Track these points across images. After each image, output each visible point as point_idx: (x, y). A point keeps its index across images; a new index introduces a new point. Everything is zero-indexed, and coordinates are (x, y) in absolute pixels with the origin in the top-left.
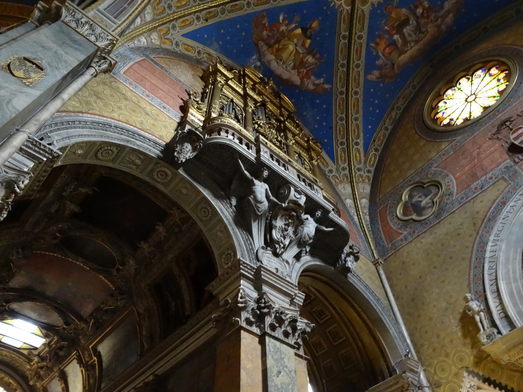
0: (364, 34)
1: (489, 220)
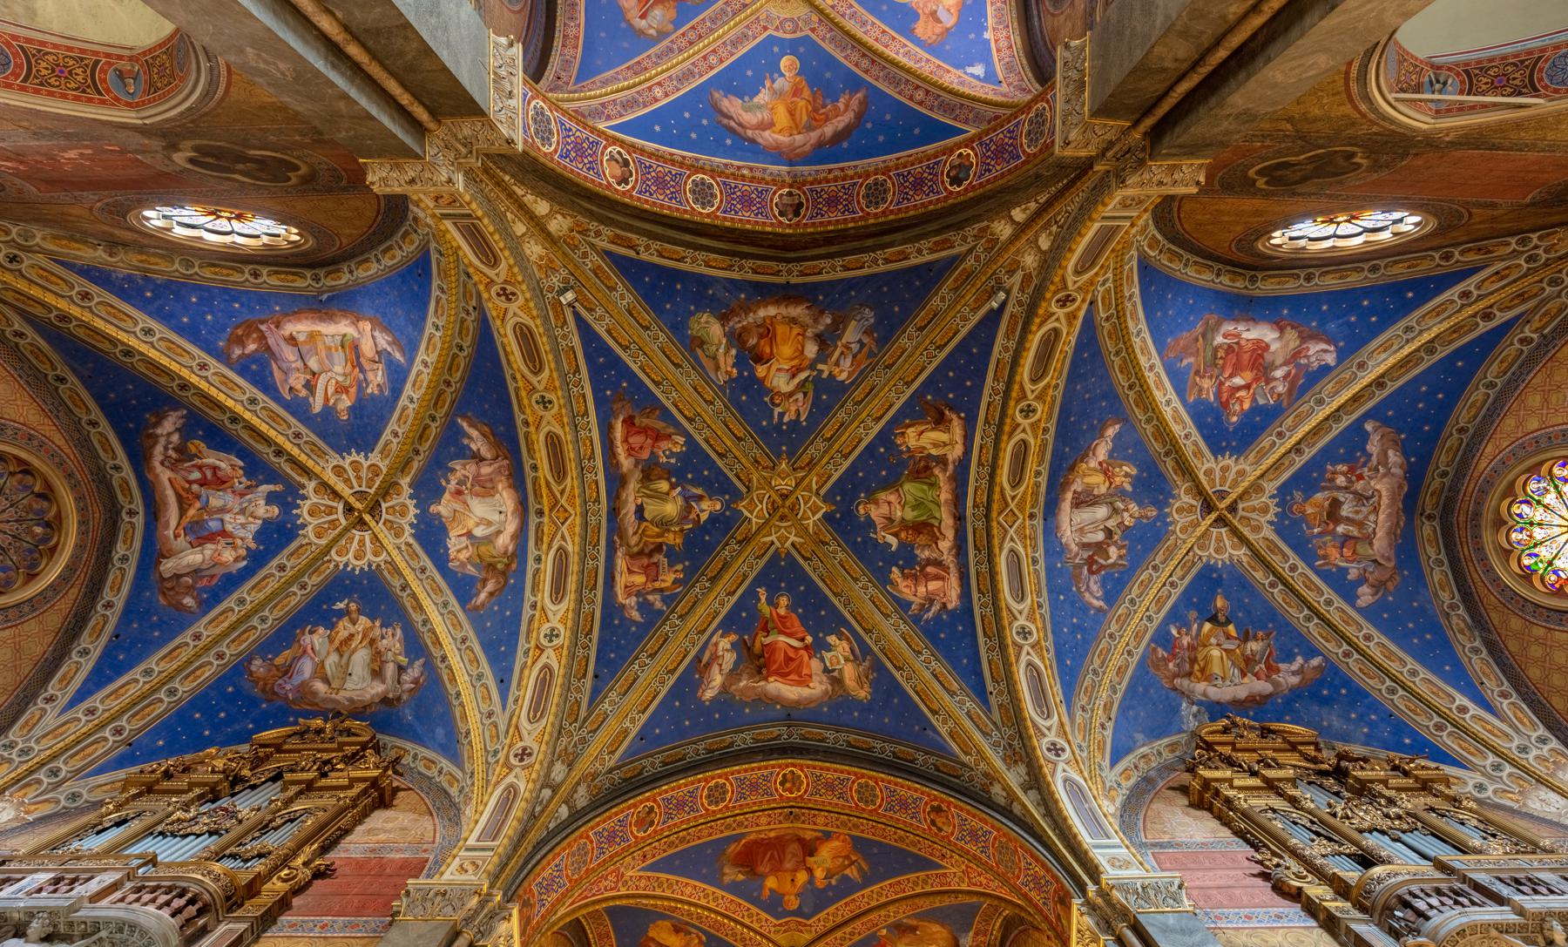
0: (1294, 559)
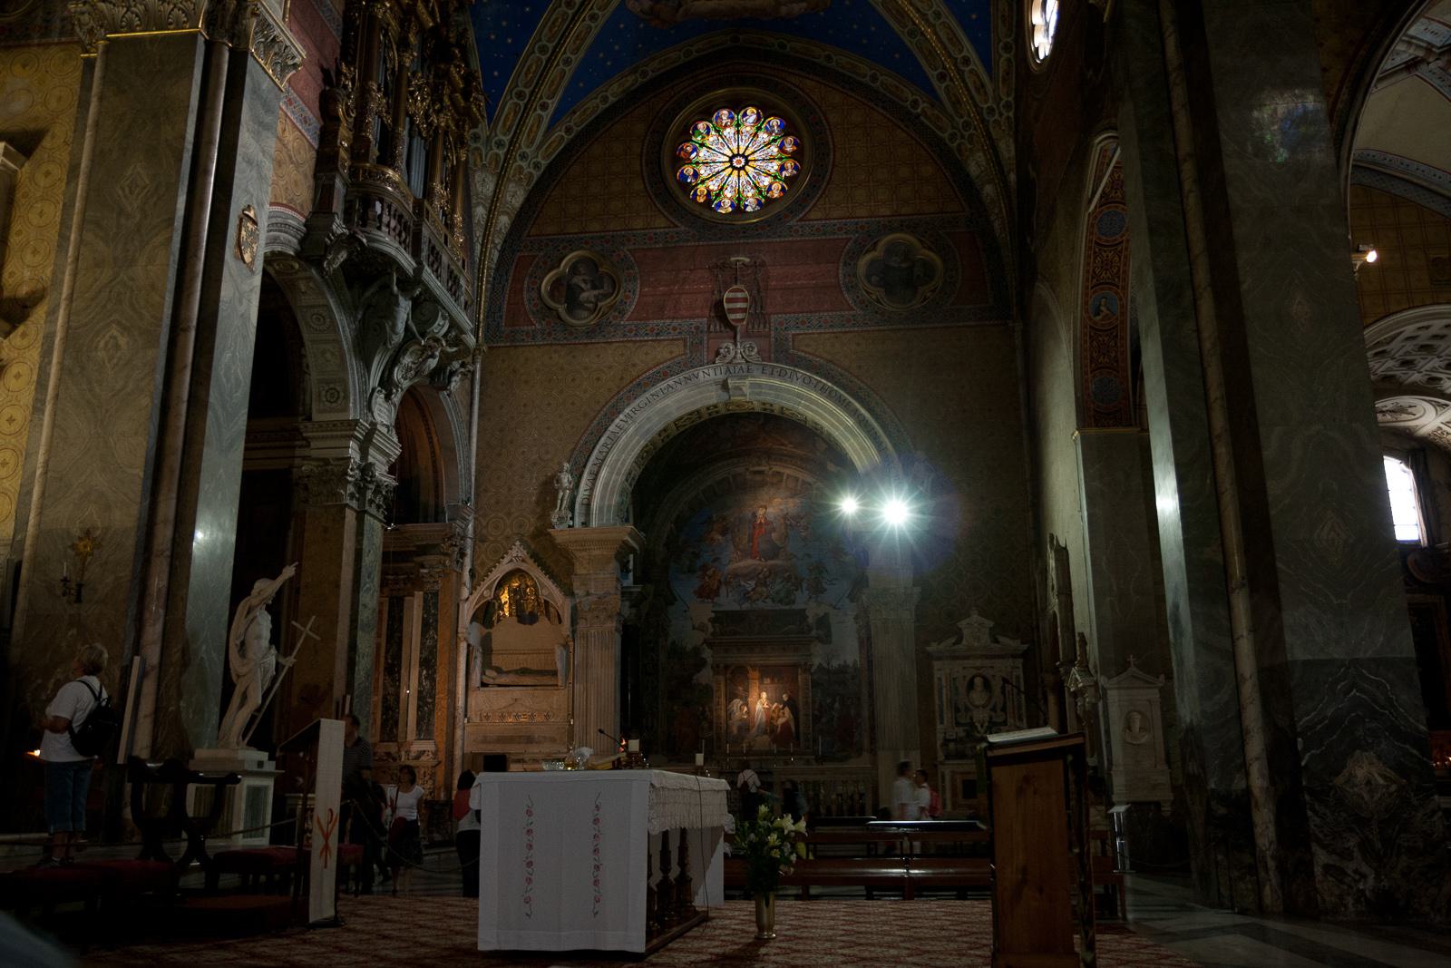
1: (639, 384)
